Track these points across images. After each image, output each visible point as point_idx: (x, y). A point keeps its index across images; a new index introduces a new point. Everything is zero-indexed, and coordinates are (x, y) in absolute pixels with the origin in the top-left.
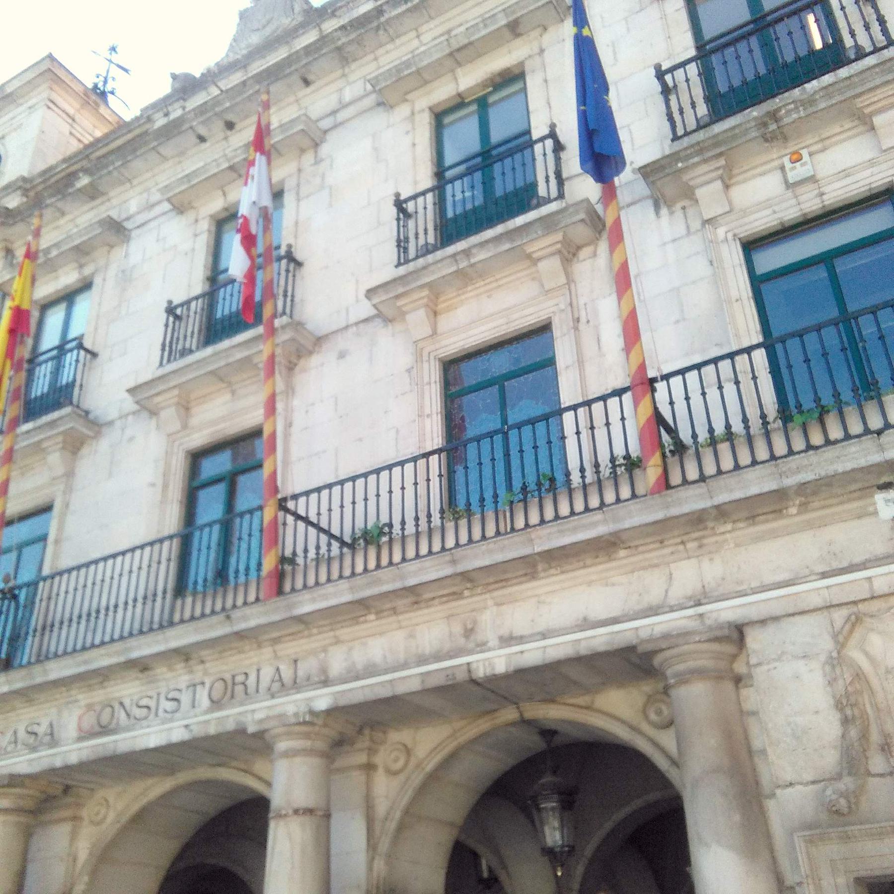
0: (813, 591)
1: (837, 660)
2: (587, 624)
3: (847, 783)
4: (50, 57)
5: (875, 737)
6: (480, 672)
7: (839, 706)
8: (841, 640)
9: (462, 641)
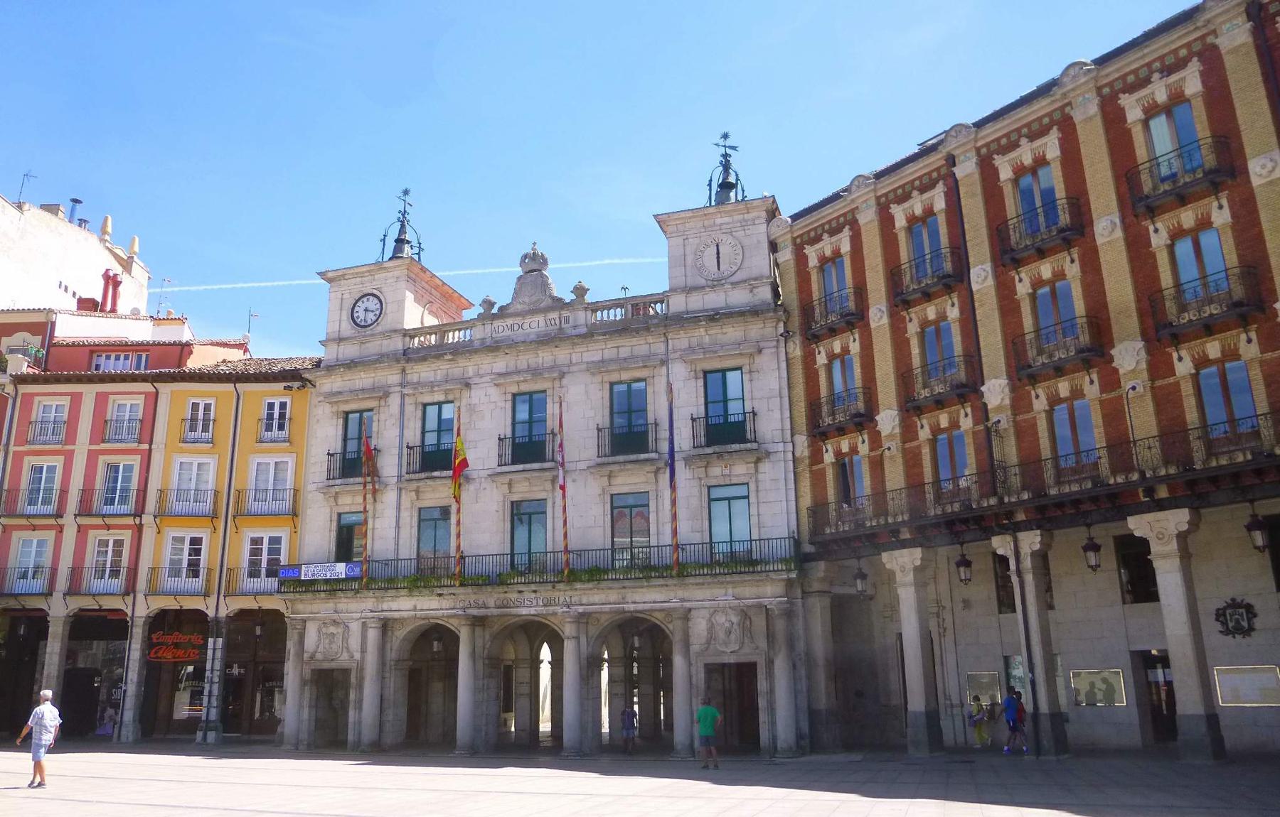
0: (707, 604)
1: (709, 620)
8: (711, 615)
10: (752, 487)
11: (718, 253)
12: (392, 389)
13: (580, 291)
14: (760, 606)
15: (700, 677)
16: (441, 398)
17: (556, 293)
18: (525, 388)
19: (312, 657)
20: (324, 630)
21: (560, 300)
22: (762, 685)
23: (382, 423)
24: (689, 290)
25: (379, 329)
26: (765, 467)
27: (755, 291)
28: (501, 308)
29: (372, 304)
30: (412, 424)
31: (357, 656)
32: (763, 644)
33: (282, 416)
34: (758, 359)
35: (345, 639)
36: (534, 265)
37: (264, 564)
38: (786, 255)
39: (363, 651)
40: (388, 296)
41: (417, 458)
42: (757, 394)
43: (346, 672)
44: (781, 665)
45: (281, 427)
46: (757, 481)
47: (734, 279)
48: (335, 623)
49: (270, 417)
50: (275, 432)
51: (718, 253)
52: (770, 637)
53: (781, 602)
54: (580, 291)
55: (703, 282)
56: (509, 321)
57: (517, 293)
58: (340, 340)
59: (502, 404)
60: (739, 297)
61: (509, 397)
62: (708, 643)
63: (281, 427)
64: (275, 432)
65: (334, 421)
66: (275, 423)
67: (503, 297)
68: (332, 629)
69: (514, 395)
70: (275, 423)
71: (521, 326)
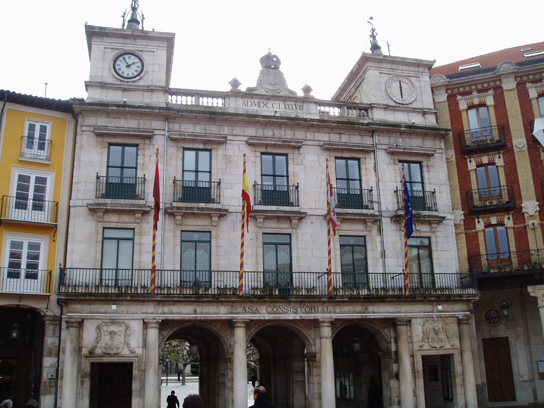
7: (423, 333)
10: (433, 240)
11: (401, 87)
13: (307, 90)
14: (453, 316)
15: (419, 366)
16: (201, 146)
18: (270, 150)
19: (91, 353)
20: (105, 328)
21: (294, 93)
22: (458, 369)
23: (147, 158)
24: (387, 107)
25: (141, 83)
26: (441, 228)
27: (426, 116)
28: (250, 90)
30: (173, 163)
32: (457, 343)
33: (42, 138)
34: (432, 159)
35: (126, 335)
37: (24, 265)
38: (442, 97)
40: (147, 58)
41: (179, 190)
42: (433, 181)
44: (468, 356)
45: (41, 147)
46: (436, 237)
48: (114, 322)
49: (31, 137)
50: (35, 150)
51: (401, 87)
53: (465, 315)
54: (307, 90)
55: (394, 104)
56: (256, 101)
57: (260, 82)
58: (103, 86)
60: (417, 120)
63: (41, 147)
64: (35, 150)
65: (99, 150)
66: (36, 141)
67: (249, 80)
68: (114, 328)
69: (262, 153)
70: (36, 141)
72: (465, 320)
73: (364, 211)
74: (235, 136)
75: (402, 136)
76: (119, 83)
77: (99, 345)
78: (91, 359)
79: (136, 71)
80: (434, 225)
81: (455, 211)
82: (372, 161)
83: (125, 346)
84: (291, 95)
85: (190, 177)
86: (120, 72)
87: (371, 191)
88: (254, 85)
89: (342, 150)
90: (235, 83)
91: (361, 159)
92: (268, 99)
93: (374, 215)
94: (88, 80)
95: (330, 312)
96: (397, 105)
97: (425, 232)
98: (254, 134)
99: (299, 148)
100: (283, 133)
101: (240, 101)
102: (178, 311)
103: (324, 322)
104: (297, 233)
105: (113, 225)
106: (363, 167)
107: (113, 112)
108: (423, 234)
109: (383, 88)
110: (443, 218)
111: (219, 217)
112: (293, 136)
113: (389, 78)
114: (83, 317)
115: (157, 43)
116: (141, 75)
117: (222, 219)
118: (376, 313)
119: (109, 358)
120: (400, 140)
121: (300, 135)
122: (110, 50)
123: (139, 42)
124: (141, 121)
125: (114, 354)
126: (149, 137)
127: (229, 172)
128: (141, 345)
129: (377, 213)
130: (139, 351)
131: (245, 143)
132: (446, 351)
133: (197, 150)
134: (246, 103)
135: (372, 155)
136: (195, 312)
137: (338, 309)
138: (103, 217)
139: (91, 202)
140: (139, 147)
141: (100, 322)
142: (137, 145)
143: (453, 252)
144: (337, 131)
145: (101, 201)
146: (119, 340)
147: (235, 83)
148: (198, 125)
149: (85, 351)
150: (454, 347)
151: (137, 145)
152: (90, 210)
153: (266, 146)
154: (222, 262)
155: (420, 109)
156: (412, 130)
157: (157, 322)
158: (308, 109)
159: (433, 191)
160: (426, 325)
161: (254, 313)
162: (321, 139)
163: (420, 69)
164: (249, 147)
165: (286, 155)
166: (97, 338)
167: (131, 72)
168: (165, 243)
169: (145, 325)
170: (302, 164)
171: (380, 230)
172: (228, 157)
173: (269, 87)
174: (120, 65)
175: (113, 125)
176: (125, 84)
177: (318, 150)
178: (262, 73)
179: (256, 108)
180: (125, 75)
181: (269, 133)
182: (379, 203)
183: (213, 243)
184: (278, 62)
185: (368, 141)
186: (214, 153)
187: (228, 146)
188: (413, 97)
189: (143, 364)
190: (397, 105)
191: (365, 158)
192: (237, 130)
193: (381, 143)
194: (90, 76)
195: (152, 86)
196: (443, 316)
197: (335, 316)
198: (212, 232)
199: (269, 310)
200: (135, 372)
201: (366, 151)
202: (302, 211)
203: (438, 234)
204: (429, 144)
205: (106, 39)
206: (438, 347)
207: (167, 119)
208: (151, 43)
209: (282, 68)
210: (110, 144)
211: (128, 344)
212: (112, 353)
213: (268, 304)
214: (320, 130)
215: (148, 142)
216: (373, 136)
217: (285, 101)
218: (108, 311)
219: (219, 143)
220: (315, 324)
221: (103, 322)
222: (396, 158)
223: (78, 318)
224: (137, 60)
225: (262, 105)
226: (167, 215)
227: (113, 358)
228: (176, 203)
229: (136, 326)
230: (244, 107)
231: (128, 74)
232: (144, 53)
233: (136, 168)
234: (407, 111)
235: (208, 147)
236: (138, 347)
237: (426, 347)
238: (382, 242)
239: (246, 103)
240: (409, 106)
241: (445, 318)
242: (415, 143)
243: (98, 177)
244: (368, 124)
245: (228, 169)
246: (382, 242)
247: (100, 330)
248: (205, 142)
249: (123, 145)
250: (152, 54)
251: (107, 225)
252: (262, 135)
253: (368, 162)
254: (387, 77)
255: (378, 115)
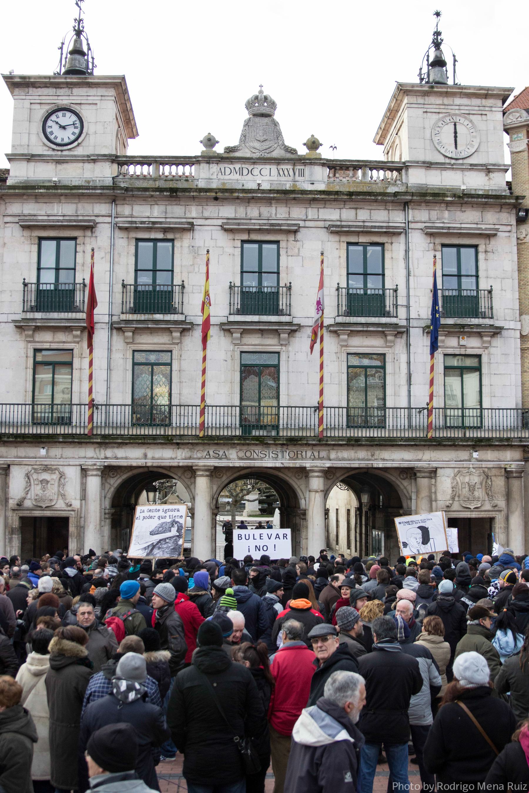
0: (453, 464)
2: (403, 460)
3: (451, 502)
4: (123, 78)
5: (457, 494)
6: (375, 466)
7: (453, 488)
9: (370, 457)
10: (484, 359)
11: (456, 133)
12: (98, 220)
13: (313, 145)
16: (160, 236)
17: (289, 142)
19: (20, 504)
20: (35, 476)
21: (293, 151)
24: (429, 165)
25: (79, 151)
26: (497, 342)
27: (492, 175)
29: (68, 119)
31: (76, 504)
32: (502, 503)
34: (493, 241)
36: (261, 110)
39: (84, 497)
42: (491, 273)
43: (64, 521)
47: (473, 161)
48: (46, 469)
51: (456, 133)
52: (508, 496)
54: (313, 145)
55: (442, 160)
56: (238, 166)
57: (244, 137)
58: (31, 158)
59: (230, 250)
60: (475, 182)
61: (239, 244)
62: (453, 499)
65: (27, 247)
67: (228, 137)
68: (45, 476)
69: (243, 242)
71: (250, 172)
72: (516, 472)
73: (384, 320)
74: (207, 219)
75: (449, 208)
76: (50, 153)
77: (29, 496)
78: (19, 512)
79: (73, 133)
80: (485, 339)
81: (524, 316)
82: (402, 247)
83: (60, 497)
84: (289, 156)
85: (145, 279)
86: (52, 137)
87: (396, 291)
88: (234, 142)
89: (358, 233)
90: (210, 142)
91: (386, 245)
92: (254, 163)
93: (396, 325)
94: (9, 152)
95: (322, 459)
96: (448, 161)
97: (473, 348)
98: (232, 216)
99: (295, 232)
100: (274, 212)
101: (214, 168)
102: (124, 456)
103: (313, 471)
104: (288, 352)
105: (47, 346)
106: (387, 255)
107: (42, 195)
108: (469, 352)
109: (428, 136)
110: (501, 328)
111: (181, 333)
112: (287, 216)
113: (439, 120)
114: (9, 463)
115: (101, 91)
116: (80, 140)
117: (186, 334)
118: (387, 460)
119: (41, 512)
120: (446, 214)
121: (297, 212)
122: (37, 107)
123: (76, 91)
124: (80, 205)
125: (46, 507)
126: (90, 227)
127: (196, 270)
128: (78, 497)
129: (404, 323)
130: (76, 504)
131: (220, 228)
132: (483, 513)
133: (155, 241)
134: (223, 170)
135: (402, 238)
136: (145, 456)
137: (333, 455)
138: (33, 336)
139: (18, 317)
140: (78, 241)
141: (30, 468)
142: (75, 239)
143: (513, 376)
144: (352, 205)
145: (30, 315)
146: (52, 491)
147: (210, 142)
148: (156, 206)
149: (12, 503)
150: (496, 509)
151: (75, 239)
152: (17, 327)
153: (249, 231)
154: (185, 391)
155: (481, 165)
156: (464, 199)
157: (97, 469)
158: (311, 175)
159: (489, 288)
160: (457, 478)
161: (221, 459)
162: (327, 217)
163: (489, 102)
164: (225, 234)
165: (277, 242)
166: (26, 488)
167: (66, 136)
168: (112, 368)
169: (84, 472)
170: (298, 255)
171: (408, 345)
172: (196, 249)
173: (257, 145)
174: (51, 127)
175: (43, 213)
176: (60, 153)
177: (323, 234)
178: (247, 124)
179: (237, 176)
180: (59, 141)
181: (253, 211)
182: (408, 307)
183: (175, 366)
184: (273, 105)
185: (397, 218)
186: (177, 244)
187: (197, 234)
188: (473, 146)
189: (83, 519)
190: (448, 161)
191: (392, 243)
192: (211, 210)
193: (417, 219)
194: (13, 146)
195: (93, 155)
196: (483, 466)
197: (328, 464)
198: (174, 352)
199: (241, 454)
200: (72, 529)
201: (392, 233)
202: (296, 321)
203: (492, 350)
204: (491, 219)
205: (32, 90)
206: (472, 507)
207: (114, 201)
208: (92, 91)
209: (277, 117)
210: (41, 239)
211: (63, 496)
212: (44, 506)
213: (238, 447)
214: (327, 206)
215: (89, 233)
216: (405, 210)
217: (278, 164)
218: (38, 456)
219: (184, 230)
220: (303, 473)
221: (33, 469)
222: (439, 241)
223: (3, 464)
224: (74, 118)
225: (245, 172)
226: (115, 331)
227: (45, 512)
228: (124, 315)
229: (73, 474)
230: (220, 176)
231: (63, 139)
232: (83, 107)
233: (75, 269)
234: (463, 170)
235: (170, 236)
236: (76, 499)
237: (456, 506)
238: (409, 363)
239: (223, 170)
240: (466, 161)
241: (486, 470)
242: (468, 219)
243: (25, 285)
244: (396, 194)
245: (196, 266)
246: (409, 363)
247: (29, 478)
248: (165, 230)
249: (58, 239)
250: (94, 107)
251: (39, 346)
252: (243, 216)
253: (396, 250)
254: (435, 117)
255: (417, 178)
